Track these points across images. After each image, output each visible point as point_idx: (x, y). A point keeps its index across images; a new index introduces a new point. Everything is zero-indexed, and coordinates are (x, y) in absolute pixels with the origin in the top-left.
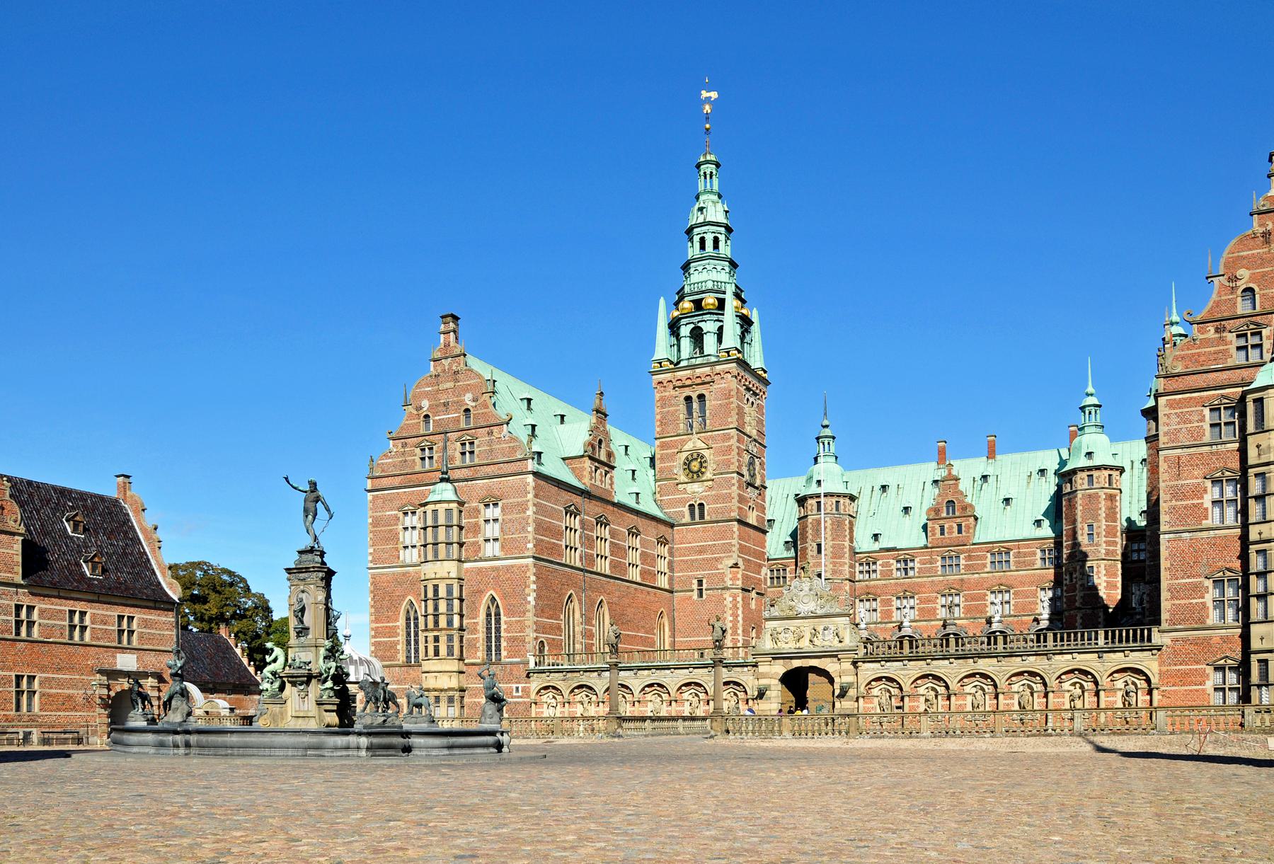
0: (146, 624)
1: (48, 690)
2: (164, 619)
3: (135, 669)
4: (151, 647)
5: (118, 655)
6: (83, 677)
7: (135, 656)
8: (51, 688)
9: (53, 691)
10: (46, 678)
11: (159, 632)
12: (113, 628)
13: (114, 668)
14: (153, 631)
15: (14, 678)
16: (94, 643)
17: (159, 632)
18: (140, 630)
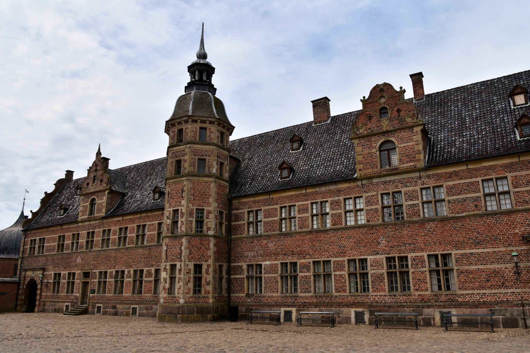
1: (466, 267)
8: (471, 264)
9: (474, 267)
10: (462, 255)
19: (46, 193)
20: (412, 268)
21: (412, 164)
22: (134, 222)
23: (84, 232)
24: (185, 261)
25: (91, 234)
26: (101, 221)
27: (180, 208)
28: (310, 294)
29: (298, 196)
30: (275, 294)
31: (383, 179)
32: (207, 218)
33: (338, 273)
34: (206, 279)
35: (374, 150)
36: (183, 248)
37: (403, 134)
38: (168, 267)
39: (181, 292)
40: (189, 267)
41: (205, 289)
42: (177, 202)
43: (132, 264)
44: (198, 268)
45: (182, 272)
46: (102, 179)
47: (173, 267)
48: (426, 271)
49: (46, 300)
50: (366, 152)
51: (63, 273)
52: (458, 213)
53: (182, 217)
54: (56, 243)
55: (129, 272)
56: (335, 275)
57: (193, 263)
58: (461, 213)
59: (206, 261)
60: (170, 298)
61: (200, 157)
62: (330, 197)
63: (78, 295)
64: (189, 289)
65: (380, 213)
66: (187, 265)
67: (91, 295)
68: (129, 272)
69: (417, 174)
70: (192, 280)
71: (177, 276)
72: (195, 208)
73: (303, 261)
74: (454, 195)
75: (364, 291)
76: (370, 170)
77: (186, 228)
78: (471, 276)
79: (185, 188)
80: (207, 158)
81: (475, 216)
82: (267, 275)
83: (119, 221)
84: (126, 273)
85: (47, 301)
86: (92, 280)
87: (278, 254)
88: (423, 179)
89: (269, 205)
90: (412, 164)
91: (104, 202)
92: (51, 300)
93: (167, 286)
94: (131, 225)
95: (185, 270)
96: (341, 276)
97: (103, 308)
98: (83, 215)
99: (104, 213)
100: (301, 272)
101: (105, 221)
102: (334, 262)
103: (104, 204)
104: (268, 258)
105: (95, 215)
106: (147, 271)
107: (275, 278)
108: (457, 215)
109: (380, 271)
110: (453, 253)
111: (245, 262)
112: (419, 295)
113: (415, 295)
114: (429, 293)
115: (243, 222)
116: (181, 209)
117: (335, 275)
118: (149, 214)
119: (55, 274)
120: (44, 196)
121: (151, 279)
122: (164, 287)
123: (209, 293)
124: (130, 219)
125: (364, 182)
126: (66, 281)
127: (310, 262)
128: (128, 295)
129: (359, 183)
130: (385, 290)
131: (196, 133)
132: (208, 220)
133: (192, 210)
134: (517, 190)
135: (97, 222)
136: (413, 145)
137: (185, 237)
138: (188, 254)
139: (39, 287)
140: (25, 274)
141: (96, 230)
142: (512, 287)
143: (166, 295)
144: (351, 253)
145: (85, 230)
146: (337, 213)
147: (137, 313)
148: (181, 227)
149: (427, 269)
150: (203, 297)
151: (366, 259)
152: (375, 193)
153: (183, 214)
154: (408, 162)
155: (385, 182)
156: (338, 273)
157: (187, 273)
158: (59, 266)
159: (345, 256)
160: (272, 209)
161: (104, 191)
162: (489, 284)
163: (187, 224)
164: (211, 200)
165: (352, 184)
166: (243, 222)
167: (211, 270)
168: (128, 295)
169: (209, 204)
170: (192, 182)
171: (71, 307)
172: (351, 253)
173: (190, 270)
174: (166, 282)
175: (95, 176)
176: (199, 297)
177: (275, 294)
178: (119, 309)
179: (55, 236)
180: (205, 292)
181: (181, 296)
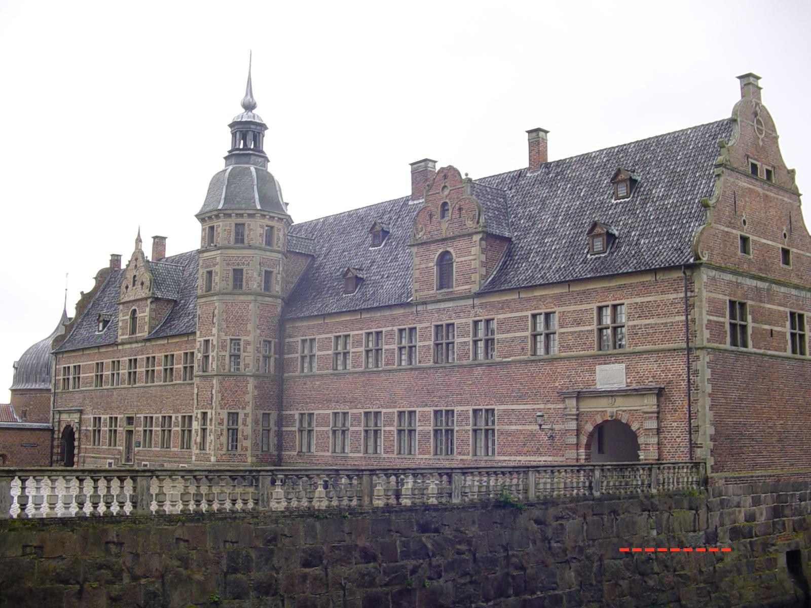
0: (641, 311)
1: (506, 427)
2: (671, 296)
3: (623, 386)
4: (649, 347)
5: (598, 368)
6: (549, 406)
7: (623, 366)
8: (511, 423)
9: (513, 427)
10: (504, 411)
11: (664, 320)
12: (589, 328)
13: (592, 389)
15: (471, 413)
16: (563, 354)
17: (664, 320)
18: (631, 323)
19: (82, 293)
20: (457, 426)
21: (467, 287)
23: (125, 359)
24: (215, 409)
25: (133, 362)
26: (143, 344)
27: (210, 338)
28: (361, 455)
30: (326, 454)
31: (438, 306)
32: (244, 352)
33: (387, 428)
34: (243, 432)
35: (431, 264)
36: (214, 392)
37: (462, 243)
38: (199, 416)
39: (212, 448)
40: (221, 417)
41: (242, 445)
42: (207, 330)
44: (233, 416)
45: (213, 423)
47: (205, 414)
48: (469, 430)
49: (86, 455)
50: (424, 266)
51: (103, 417)
52: (505, 357)
53: (213, 351)
54: (94, 374)
55: (177, 418)
56: (384, 431)
57: (226, 411)
58: (508, 357)
59: (244, 408)
60: (202, 455)
61: (235, 267)
62: (385, 326)
63: (121, 448)
64: (221, 445)
65: (432, 351)
66: (219, 414)
67: (136, 449)
68: (177, 418)
69: (470, 302)
70: (225, 432)
71: (209, 427)
72: (228, 338)
73: (354, 411)
75: (410, 454)
76: (426, 293)
77: (217, 366)
78: (510, 438)
79: (216, 312)
80: (244, 268)
81: (520, 362)
82: (318, 429)
83: (164, 345)
84: (173, 419)
86: (137, 429)
88: (476, 309)
89: (323, 333)
90: (467, 287)
91: (146, 316)
93: (199, 440)
94: (177, 353)
95: (215, 420)
96: (390, 432)
98: (123, 334)
99: (147, 333)
100: (352, 425)
101: (148, 344)
102: (385, 413)
103: (147, 319)
104: (320, 406)
107: (327, 432)
108: (504, 360)
109: (427, 428)
110: (496, 409)
111: (297, 409)
112: (461, 460)
113: (457, 460)
114: (469, 457)
115: (296, 355)
116: (212, 340)
117: (384, 431)
119: (95, 418)
120: (79, 297)
122: (195, 441)
123: (247, 450)
125: (420, 308)
126: (107, 429)
127: (361, 413)
128: (176, 449)
129: (414, 309)
130: (429, 453)
131: (229, 233)
132: (246, 354)
133: (225, 341)
135: (140, 345)
136: (470, 260)
137: (215, 377)
138: (220, 399)
139: (76, 436)
140: (59, 418)
141: (138, 357)
142: (545, 455)
143: (198, 451)
144: (402, 403)
145: (126, 356)
148: (212, 364)
149: (470, 428)
150: (240, 455)
151: (415, 412)
152: (428, 324)
153: (213, 346)
154: (463, 284)
155: (439, 310)
156: (387, 428)
157: (219, 424)
158: (99, 407)
159: (395, 407)
161: (146, 299)
162: (525, 449)
163: (218, 360)
164: (250, 327)
165: (407, 310)
166: (296, 355)
167: (249, 420)
168: (176, 449)
169: (247, 333)
170: (224, 303)
172: (402, 403)
173: (222, 420)
174: (197, 435)
175: (135, 276)
176: (234, 455)
177: (326, 454)
179: (91, 362)
180: (242, 449)
181: (213, 453)
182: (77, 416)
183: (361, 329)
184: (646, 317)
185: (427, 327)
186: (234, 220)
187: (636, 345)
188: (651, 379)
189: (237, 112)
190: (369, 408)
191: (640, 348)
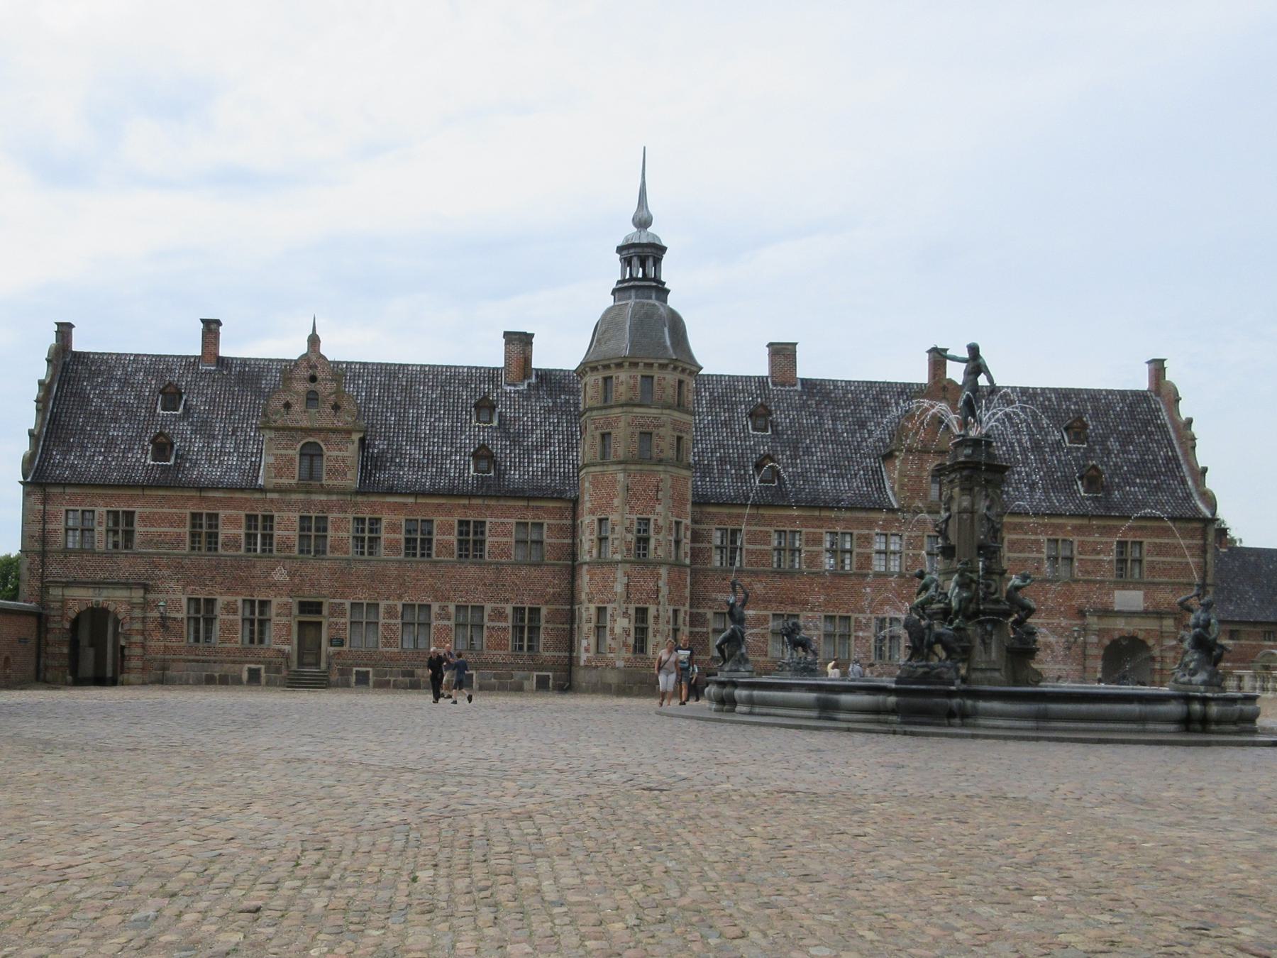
4: (1166, 579)
5: (1117, 592)
7: (1142, 592)
14: (1169, 559)
22: (450, 513)
29: (806, 518)
43: (452, 593)
46: (338, 403)
49: (167, 657)
62: (857, 528)
63: (287, 648)
74: (1015, 552)
83: (405, 504)
85: (173, 661)
87: (770, 601)
89: (756, 525)
92: (191, 657)
97: (374, 675)
105: (324, 482)
106: (494, 610)
111: (710, 608)
118: (493, 503)
121: (503, 624)
124: (440, 505)
134: (1081, 557)
135: (334, 497)
146: (863, 553)
147: (474, 684)
152: (920, 533)
160: (761, 532)
161: (349, 432)
171: (266, 672)
178: (423, 677)
182: (138, 595)
183: (821, 527)
184: (1164, 556)
185: (917, 537)
186: (639, 373)
187: (1154, 576)
188: (1166, 606)
189: (626, 231)
190: (833, 611)
191: (1157, 580)
